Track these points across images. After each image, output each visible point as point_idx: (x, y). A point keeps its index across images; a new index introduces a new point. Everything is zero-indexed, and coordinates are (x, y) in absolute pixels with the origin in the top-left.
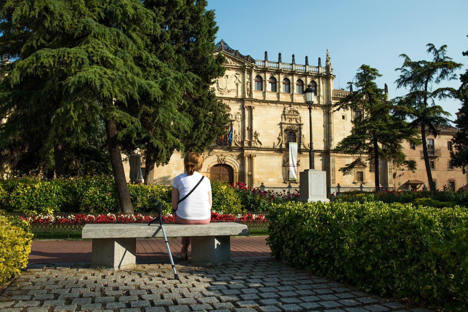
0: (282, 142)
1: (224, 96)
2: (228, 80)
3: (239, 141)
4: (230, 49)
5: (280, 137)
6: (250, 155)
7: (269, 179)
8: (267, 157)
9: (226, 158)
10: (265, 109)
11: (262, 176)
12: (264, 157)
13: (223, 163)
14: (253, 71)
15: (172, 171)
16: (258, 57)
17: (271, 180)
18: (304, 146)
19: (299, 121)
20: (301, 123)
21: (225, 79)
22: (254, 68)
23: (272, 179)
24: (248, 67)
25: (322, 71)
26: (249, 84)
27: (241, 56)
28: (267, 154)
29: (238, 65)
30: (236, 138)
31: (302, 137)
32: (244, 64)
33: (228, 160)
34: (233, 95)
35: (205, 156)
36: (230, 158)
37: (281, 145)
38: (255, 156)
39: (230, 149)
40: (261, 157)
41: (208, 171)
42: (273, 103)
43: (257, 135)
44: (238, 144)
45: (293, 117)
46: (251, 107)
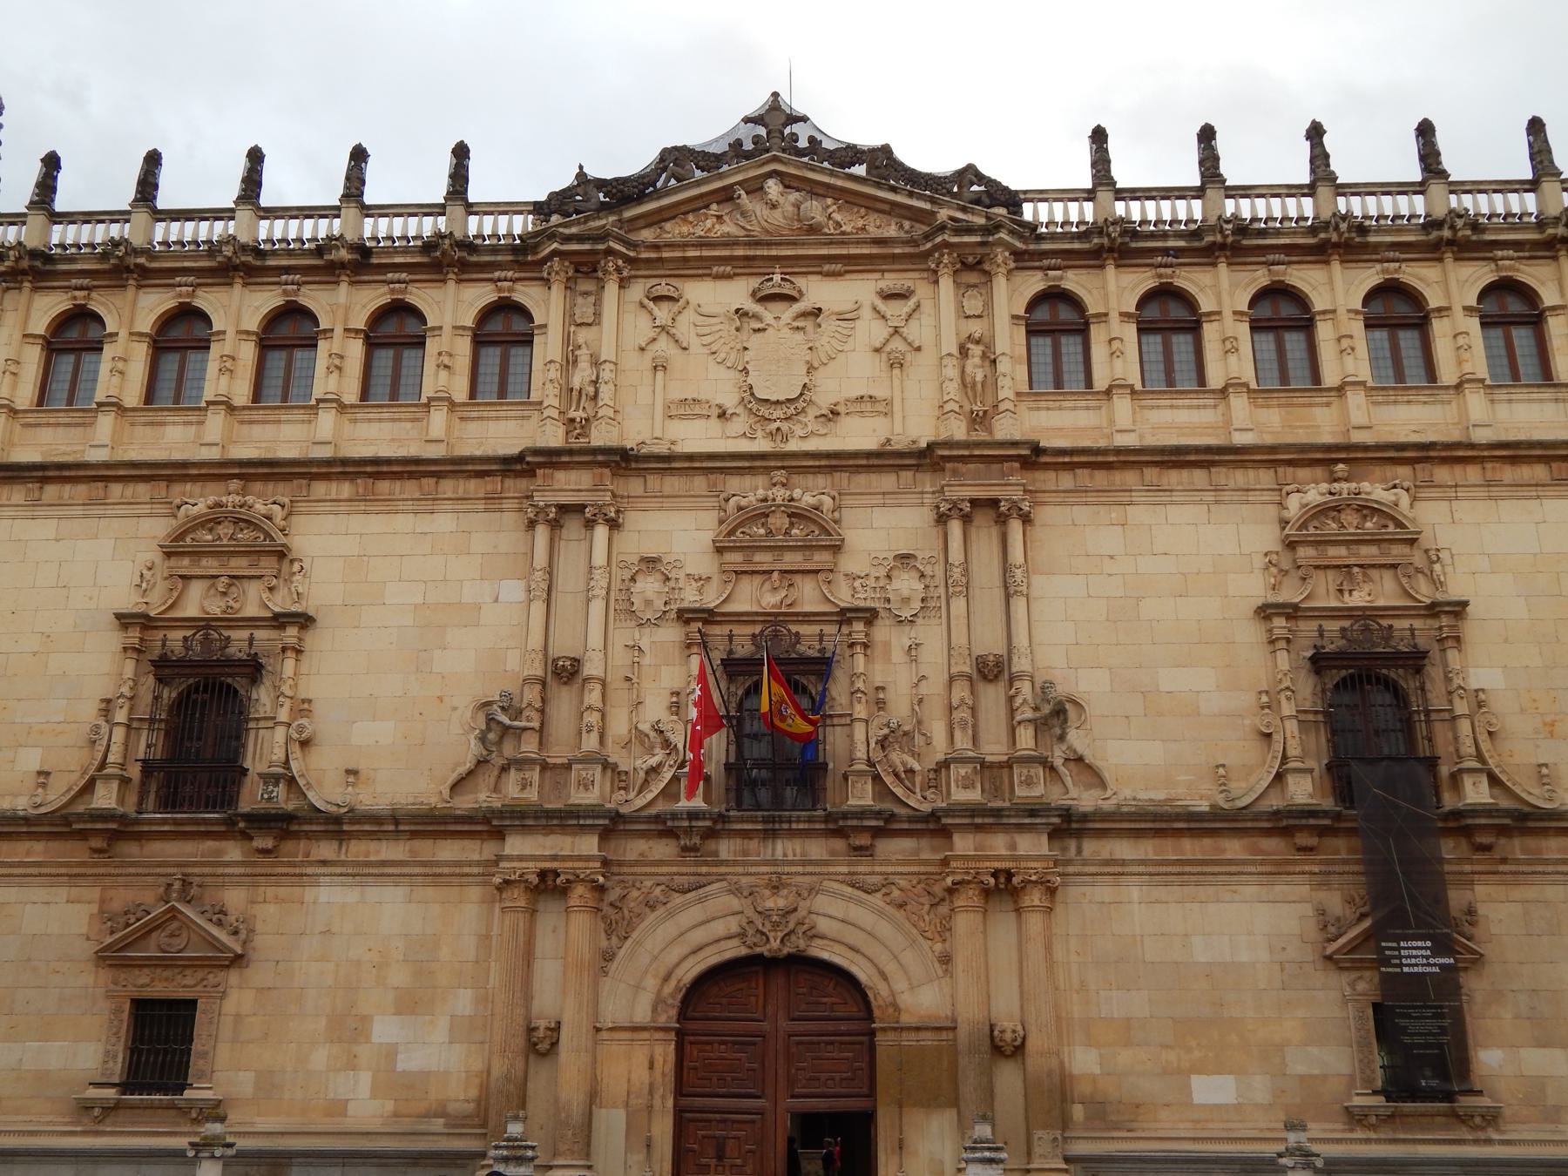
0: (1285, 757)
1: (793, 446)
3: (910, 771)
4: (827, 145)
6: (1009, 875)
7: (1196, 1081)
8: (1159, 892)
10: (1115, 513)
11: (1125, 1057)
12: (1134, 892)
14: (1001, 255)
15: (366, 1019)
16: (1039, 162)
17: (1212, 1090)
18: (1494, 780)
20: (1440, 597)
21: (799, 336)
22: (1003, 235)
23: (1228, 1081)
27: (916, 179)
28: (1159, 872)
29: (892, 231)
31: (1461, 707)
33: (823, 925)
34: (858, 435)
37: (1279, 777)
41: (662, 1020)
43: (1059, 712)
44: (899, 791)
45: (1368, 553)
46: (994, 503)
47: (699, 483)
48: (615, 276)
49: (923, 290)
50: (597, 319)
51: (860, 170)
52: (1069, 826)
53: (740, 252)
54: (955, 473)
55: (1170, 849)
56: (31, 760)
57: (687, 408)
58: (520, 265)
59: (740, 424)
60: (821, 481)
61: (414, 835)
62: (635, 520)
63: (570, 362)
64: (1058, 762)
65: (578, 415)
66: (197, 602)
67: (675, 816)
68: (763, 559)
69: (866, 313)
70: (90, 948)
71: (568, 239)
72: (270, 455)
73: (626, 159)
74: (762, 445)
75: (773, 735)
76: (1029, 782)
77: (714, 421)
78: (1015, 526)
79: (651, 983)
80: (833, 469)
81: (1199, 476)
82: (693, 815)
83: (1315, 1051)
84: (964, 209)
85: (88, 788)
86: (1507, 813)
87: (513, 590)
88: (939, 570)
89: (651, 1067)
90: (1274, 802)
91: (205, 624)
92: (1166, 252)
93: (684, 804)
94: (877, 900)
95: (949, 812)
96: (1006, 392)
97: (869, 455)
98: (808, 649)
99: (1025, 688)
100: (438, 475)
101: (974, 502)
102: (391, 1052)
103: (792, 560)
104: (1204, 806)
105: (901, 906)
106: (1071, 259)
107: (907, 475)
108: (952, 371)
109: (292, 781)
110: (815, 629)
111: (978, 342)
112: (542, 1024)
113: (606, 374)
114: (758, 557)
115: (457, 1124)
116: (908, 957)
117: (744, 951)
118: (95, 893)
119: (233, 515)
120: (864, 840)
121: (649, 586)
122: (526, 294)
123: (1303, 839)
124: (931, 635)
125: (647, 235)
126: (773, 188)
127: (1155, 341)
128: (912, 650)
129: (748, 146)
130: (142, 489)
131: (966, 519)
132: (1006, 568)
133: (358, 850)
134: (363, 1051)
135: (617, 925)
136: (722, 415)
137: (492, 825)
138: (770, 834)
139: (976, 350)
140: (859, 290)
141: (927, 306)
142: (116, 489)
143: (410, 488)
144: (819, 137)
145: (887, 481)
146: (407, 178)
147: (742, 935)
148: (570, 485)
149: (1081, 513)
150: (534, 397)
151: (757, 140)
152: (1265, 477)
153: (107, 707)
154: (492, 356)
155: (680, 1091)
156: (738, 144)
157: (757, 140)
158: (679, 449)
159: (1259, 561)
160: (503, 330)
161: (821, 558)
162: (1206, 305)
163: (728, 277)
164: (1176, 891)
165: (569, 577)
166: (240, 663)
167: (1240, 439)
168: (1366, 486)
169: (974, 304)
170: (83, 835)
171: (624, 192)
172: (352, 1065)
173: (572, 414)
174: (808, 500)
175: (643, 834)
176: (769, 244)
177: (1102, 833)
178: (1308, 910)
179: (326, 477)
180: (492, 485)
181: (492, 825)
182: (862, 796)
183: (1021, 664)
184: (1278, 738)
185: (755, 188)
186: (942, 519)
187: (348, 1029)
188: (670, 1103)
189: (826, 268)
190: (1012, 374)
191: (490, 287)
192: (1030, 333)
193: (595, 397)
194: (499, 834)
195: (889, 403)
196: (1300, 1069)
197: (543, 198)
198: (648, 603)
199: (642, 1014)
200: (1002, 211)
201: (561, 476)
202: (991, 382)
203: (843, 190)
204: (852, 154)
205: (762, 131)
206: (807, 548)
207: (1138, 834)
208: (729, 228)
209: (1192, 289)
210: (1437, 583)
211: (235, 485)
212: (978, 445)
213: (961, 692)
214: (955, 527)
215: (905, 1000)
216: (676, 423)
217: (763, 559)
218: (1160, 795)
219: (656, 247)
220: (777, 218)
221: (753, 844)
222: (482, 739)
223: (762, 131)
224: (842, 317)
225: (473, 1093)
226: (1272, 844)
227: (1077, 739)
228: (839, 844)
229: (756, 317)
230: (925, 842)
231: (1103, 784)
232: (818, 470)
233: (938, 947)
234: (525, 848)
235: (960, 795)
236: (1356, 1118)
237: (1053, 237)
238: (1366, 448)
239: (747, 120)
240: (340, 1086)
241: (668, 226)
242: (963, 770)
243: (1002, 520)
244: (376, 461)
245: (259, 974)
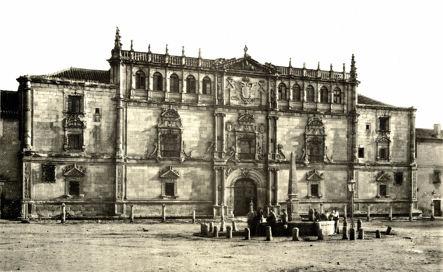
2: (252, 89)
5: (304, 150)
19: (322, 132)
21: (248, 88)
25: (347, 77)
26: (273, 92)
33: (252, 175)
36: (254, 172)
41: (232, 186)
45: (317, 127)
49: (266, 81)
63: (218, 89)
69: (258, 85)
94: (257, 171)
173: (219, 98)
210: (324, 131)
220: (247, 67)
229: (244, 84)
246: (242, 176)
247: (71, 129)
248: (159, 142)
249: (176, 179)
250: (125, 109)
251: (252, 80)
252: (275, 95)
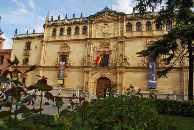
0: (144, 62)
1: (107, 37)
3: (114, 63)
4: (111, 11)
8: (133, 73)
9: (106, 74)
10: (133, 42)
12: (131, 73)
13: (104, 77)
15: (75, 81)
21: (107, 28)
22: (124, 18)
24: (120, 18)
28: (133, 71)
29: (115, 18)
30: (112, 61)
32: (118, 17)
33: (107, 75)
34: (112, 36)
35: (94, 73)
36: (108, 74)
37: (144, 64)
38: (124, 72)
39: (109, 68)
40: (129, 73)
41: (95, 82)
42: (138, 38)
44: (113, 65)
46: (122, 42)
47: (99, 41)
48: (93, 24)
49: (118, 23)
50: (92, 27)
51: (113, 13)
52: (127, 68)
53: (103, 21)
54: (119, 39)
55: (134, 70)
56: (53, 63)
57: (99, 34)
58: (86, 23)
59: (102, 36)
60: (109, 40)
61: (78, 68)
62: (94, 44)
63: (90, 31)
64: (126, 63)
65: (90, 35)
66: (63, 51)
67: (96, 67)
68: (104, 47)
69: (113, 26)
70: (57, 76)
71: (89, 21)
72: (68, 39)
73: (94, 13)
74: (104, 37)
75: (104, 61)
76: (123, 64)
77: (101, 36)
78: (124, 44)
79: (94, 79)
80: (109, 39)
81: (140, 39)
82: (97, 67)
83: (144, 85)
84: (121, 16)
85: (56, 64)
86: (162, 67)
87: (85, 49)
88: (118, 47)
89: (94, 85)
90: (143, 66)
91: (63, 53)
92: (138, 19)
93: (97, 66)
94: (111, 73)
95: (116, 67)
96: (124, 32)
97: (112, 38)
98: (107, 54)
99: (124, 57)
100: (80, 41)
101: (121, 42)
102: (77, 83)
103: (106, 47)
104: (137, 66)
105: (113, 74)
106: (130, 20)
107: (115, 39)
108: (120, 31)
109: (70, 64)
110: (107, 52)
111: (122, 28)
112: (87, 82)
113: (92, 32)
114: (103, 47)
115: (81, 88)
116: (113, 78)
117: (101, 77)
118: (57, 72)
119: (65, 44)
120: (110, 69)
121: (95, 49)
122: (86, 25)
123: (145, 69)
124: (116, 52)
125: (96, 20)
126: (106, 15)
127: (138, 27)
128: (115, 54)
129: (104, 11)
130: (59, 42)
131: (120, 43)
132: (123, 47)
133: (74, 69)
134: (75, 83)
135: (92, 75)
136: (101, 35)
137: (83, 67)
138: (103, 68)
139: (122, 28)
140: (113, 23)
141: (118, 25)
142: (57, 42)
143: (77, 42)
144: (110, 10)
145: (114, 40)
146: (78, 16)
147: (101, 76)
148: (89, 41)
149: (130, 42)
150: (87, 34)
151: (105, 11)
152: (145, 39)
153: (57, 59)
154: (84, 30)
155: (97, 87)
156: (103, 11)
157: (105, 11)
158: (98, 38)
159: (144, 46)
160: (85, 29)
161: (108, 46)
162: (142, 24)
163: (102, 23)
164: (135, 73)
165: (89, 49)
166: (66, 55)
167: (143, 36)
168: (154, 39)
169: (122, 24)
170: (56, 68)
171: (94, 16)
172: (74, 84)
174: (108, 42)
175: (94, 68)
176: (105, 20)
177: (129, 68)
178: (145, 74)
179: (72, 41)
180: (84, 41)
181: (83, 67)
182: (110, 65)
183: (124, 55)
184: (144, 61)
185: (104, 15)
186: (118, 43)
187: (74, 82)
188: (96, 87)
189: (110, 22)
190: (125, 30)
191: (84, 25)
192: (127, 27)
193: (91, 34)
194: (84, 68)
195: (115, 33)
196: (143, 87)
197: (88, 17)
198: (95, 50)
199: (94, 81)
200: (125, 16)
201: (88, 40)
202: (123, 31)
203: (112, 15)
204: (112, 12)
205: (105, 10)
206: (107, 46)
207: (132, 68)
208: (102, 19)
209: (141, 22)
211: (66, 42)
212: (122, 37)
213: (119, 57)
214: (119, 44)
215: (113, 81)
216: (98, 36)
217: (104, 47)
218: (134, 65)
219: (96, 21)
221: (102, 69)
222: (83, 61)
223: (105, 10)
224: (111, 26)
225: (82, 86)
226: (142, 69)
227: (128, 61)
228: (109, 69)
229: (104, 26)
230: (115, 69)
231: (129, 65)
232: (108, 39)
233: (116, 77)
234: (85, 69)
235: (118, 65)
236: (147, 90)
237: (129, 18)
238: (154, 36)
239: (104, 9)
240: (73, 85)
241: (98, 19)
242: (118, 63)
243: (123, 43)
244: (75, 40)
245: (68, 78)
246: (101, 76)
247: (26, 56)
248: (58, 59)
249: (65, 77)
250: (46, 46)
251: (109, 24)
252: (123, 29)
